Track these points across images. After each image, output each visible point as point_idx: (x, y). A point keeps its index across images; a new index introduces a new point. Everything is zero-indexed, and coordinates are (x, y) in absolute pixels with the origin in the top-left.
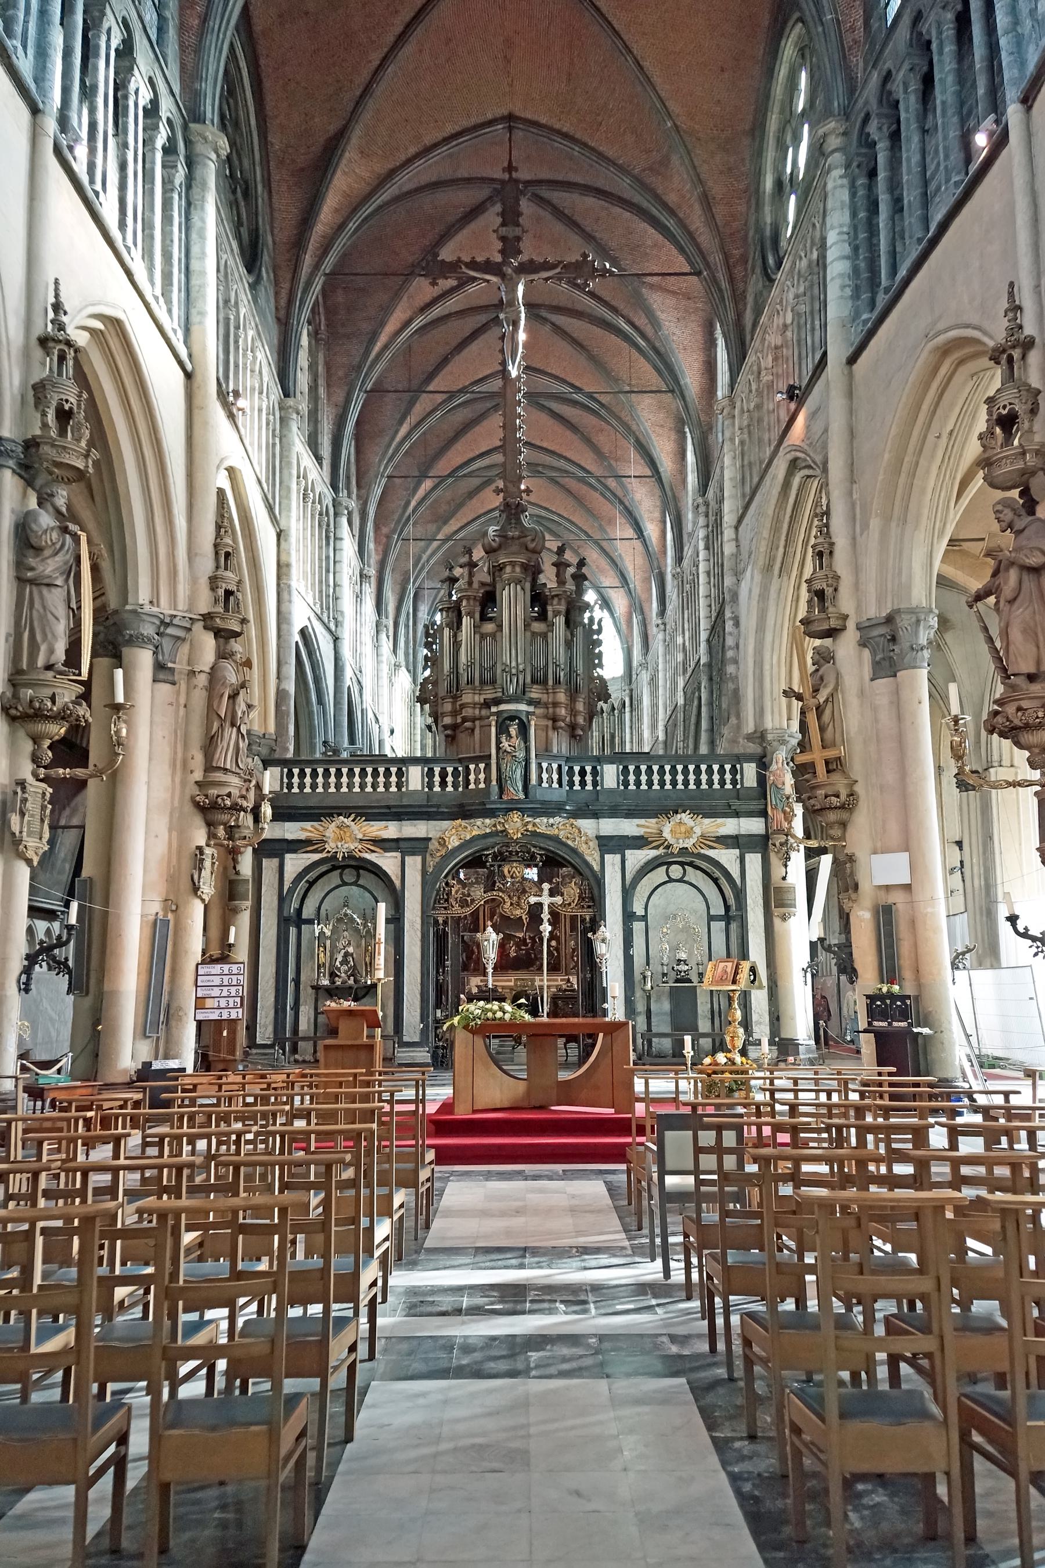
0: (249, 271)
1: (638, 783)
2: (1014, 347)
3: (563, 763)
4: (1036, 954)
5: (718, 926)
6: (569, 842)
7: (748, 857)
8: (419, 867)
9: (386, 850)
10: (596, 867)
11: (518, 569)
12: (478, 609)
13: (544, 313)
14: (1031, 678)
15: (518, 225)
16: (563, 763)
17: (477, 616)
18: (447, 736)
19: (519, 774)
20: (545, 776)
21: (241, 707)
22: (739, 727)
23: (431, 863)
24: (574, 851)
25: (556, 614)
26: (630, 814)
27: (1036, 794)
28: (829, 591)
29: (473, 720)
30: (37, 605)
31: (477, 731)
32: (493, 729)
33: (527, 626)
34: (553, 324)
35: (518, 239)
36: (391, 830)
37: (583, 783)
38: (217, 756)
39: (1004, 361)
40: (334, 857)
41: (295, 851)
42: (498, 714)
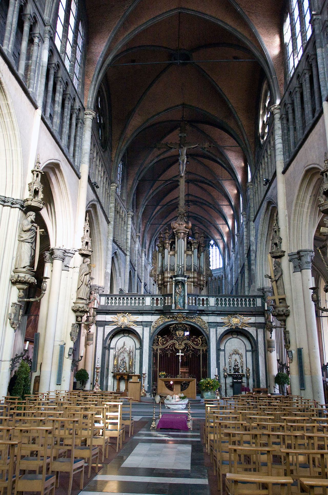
0: (103, 148)
3: (196, 297)
5: (249, 354)
6: (198, 324)
7: (259, 330)
8: (149, 331)
9: (138, 325)
11: (182, 234)
12: (170, 247)
16: (196, 297)
18: (159, 288)
20: (190, 301)
22: (255, 287)
29: (167, 282)
31: (168, 286)
32: (174, 286)
33: (185, 252)
36: (140, 318)
40: (121, 327)
41: (108, 325)
42: (175, 280)
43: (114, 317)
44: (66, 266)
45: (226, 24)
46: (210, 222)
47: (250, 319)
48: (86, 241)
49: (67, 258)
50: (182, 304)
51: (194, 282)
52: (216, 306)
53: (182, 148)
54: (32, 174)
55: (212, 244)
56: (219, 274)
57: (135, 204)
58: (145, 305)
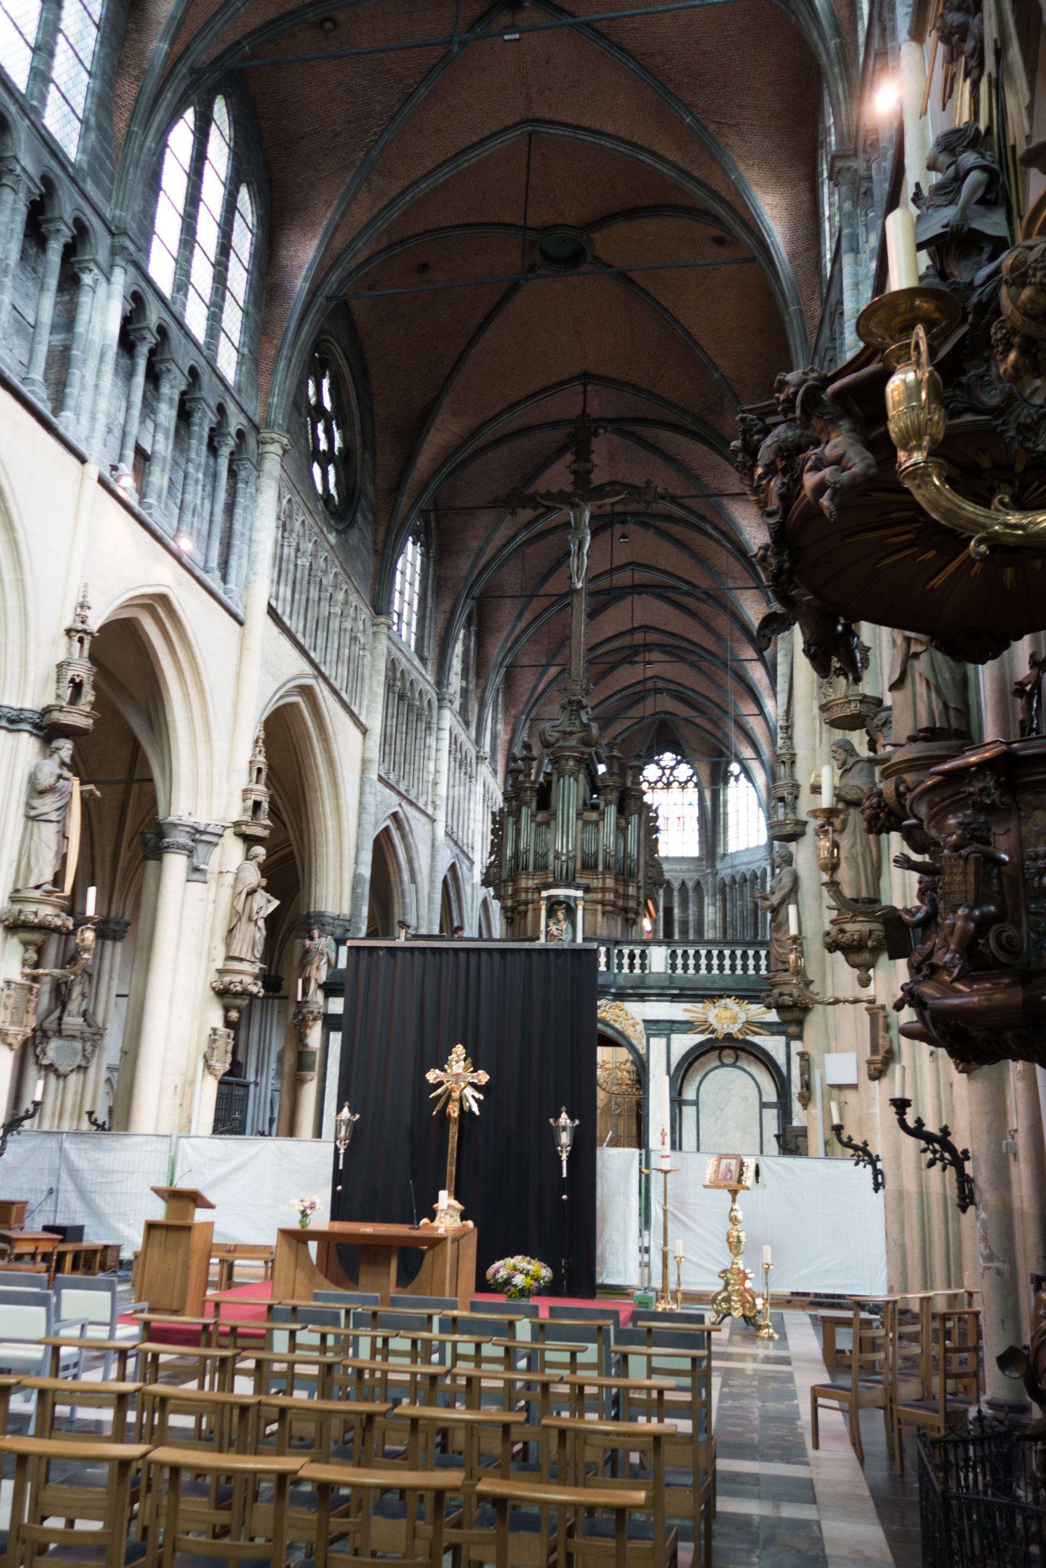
6: (617, 1025)
10: (643, 1051)
11: (571, 763)
12: (535, 799)
13: (644, 519)
15: (589, 461)
16: (611, 946)
17: (534, 805)
18: (507, 918)
24: (620, 1033)
25: (608, 803)
26: (675, 998)
27: (867, 1009)
28: (789, 798)
29: (526, 903)
30: (35, 837)
31: (530, 914)
32: (543, 913)
33: (579, 815)
34: (656, 528)
35: (589, 472)
37: (632, 967)
42: (549, 898)
45: (661, 158)
46: (720, 707)
48: (253, 797)
49: (201, 849)
51: (603, 903)
53: (578, 506)
54: (66, 639)
55: (736, 773)
56: (754, 867)
57: (472, 661)
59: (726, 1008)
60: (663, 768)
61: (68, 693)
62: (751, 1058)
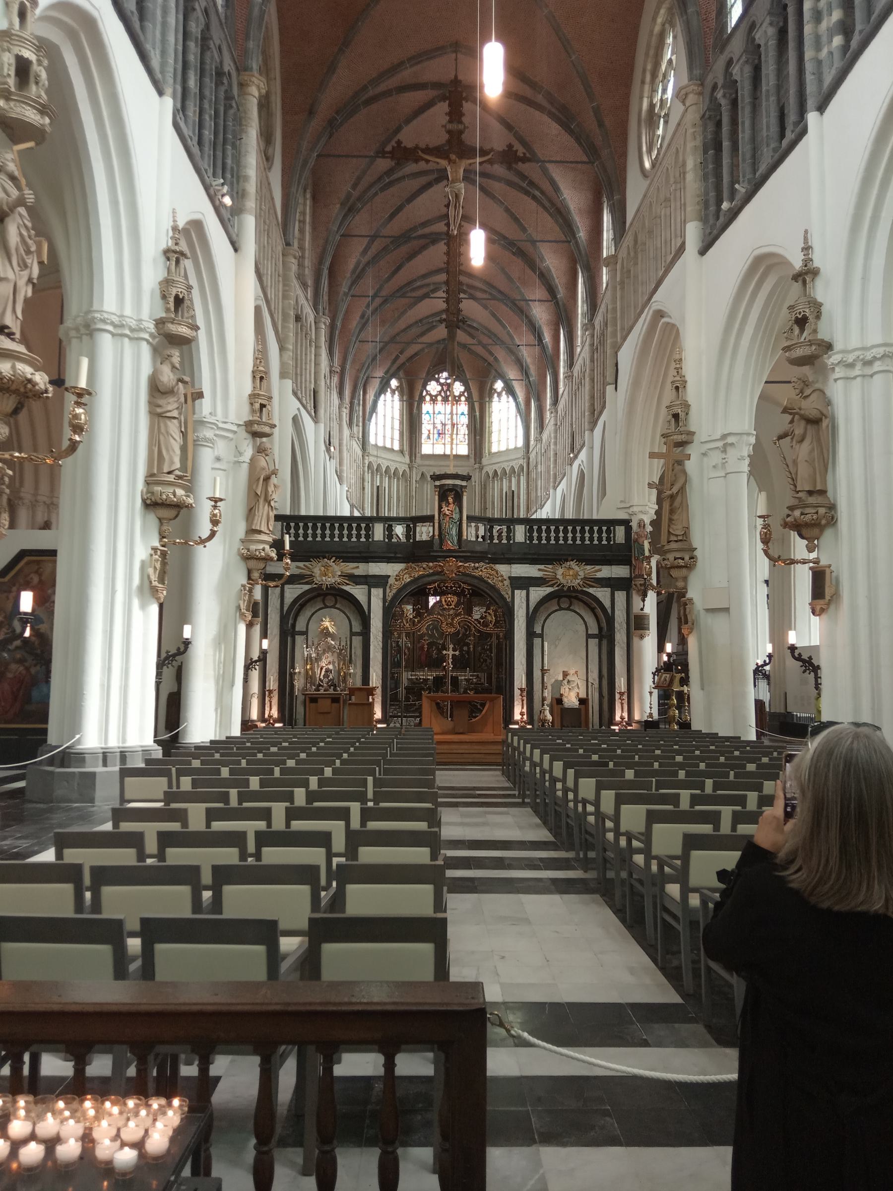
1: (540, 538)
2: (806, 273)
4: (804, 672)
5: (593, 643)
6: (489, 581)
8: (381, 596)
14: (810, 493)
15: (461, 122)
19: (454, 532)
21: (271, 489)
23: (390, 595)
24: (493, 588)
26: (533, 561)
27: (811, 568)
28: (682, 415)
38: (255, 522)
39: (800, 282)
43: (304, 565)
44: (218, 459)
47: (600, 570)
50: (455, 539)
52: (528, 542)
53: (455, 162)
55: (499, 390)
58: (373, 540)
59: (570, 568)
60: (442, 385)
61: (172, 305)
62: (581, 603)
